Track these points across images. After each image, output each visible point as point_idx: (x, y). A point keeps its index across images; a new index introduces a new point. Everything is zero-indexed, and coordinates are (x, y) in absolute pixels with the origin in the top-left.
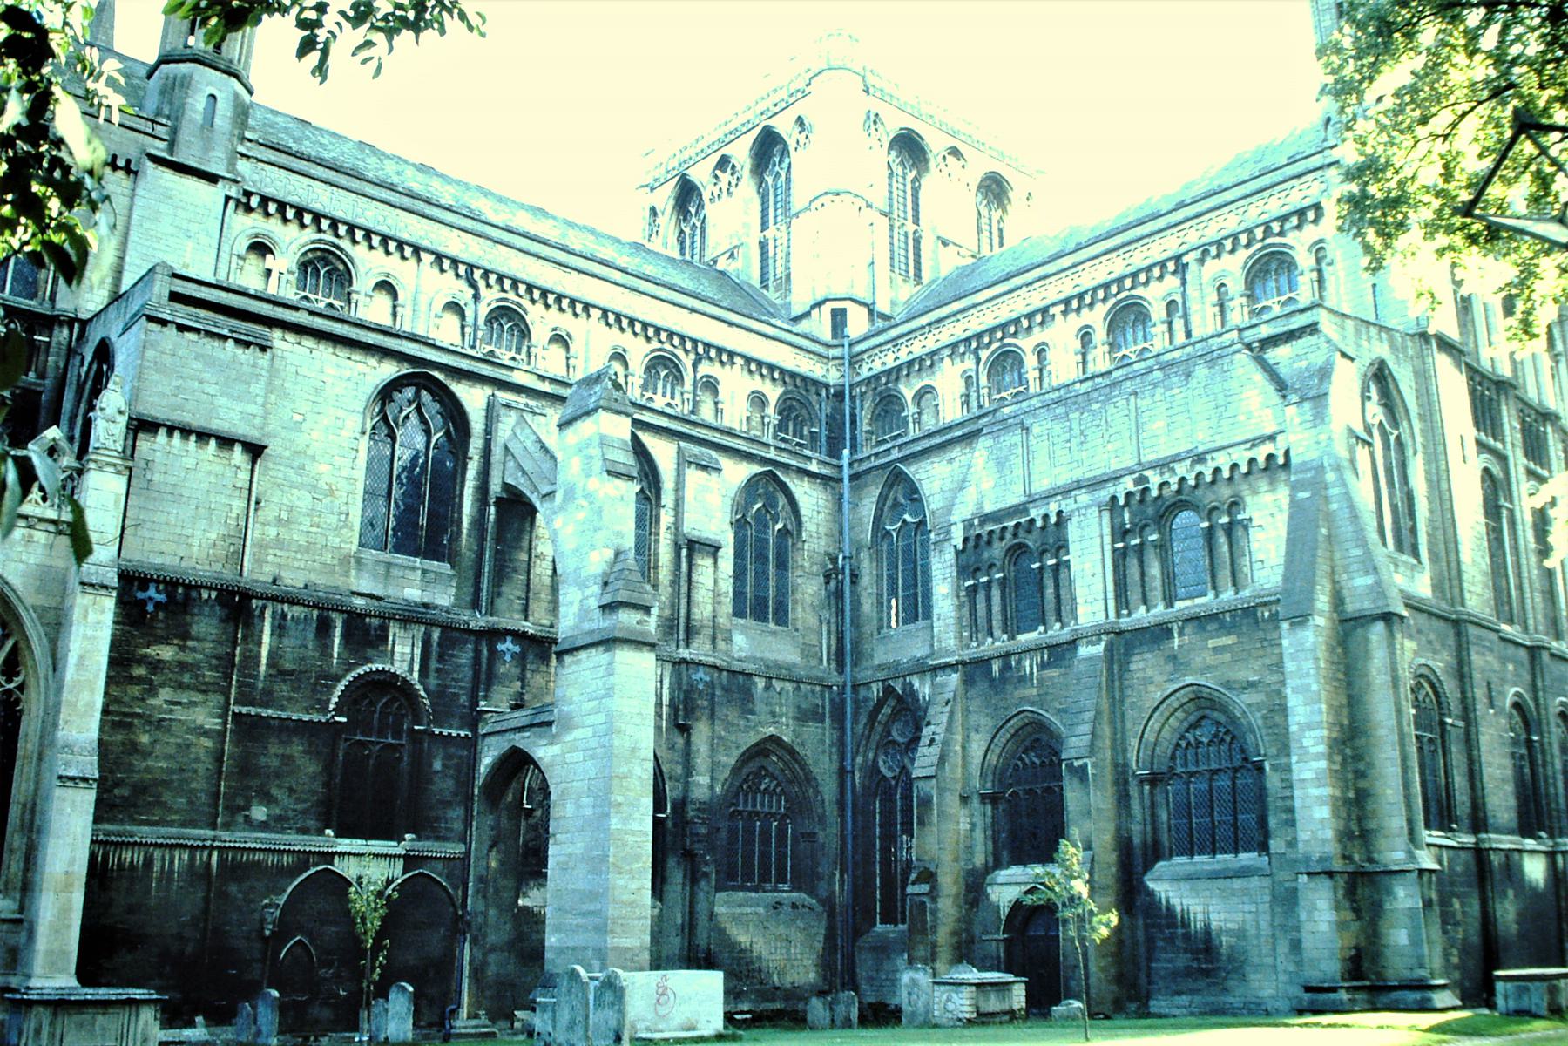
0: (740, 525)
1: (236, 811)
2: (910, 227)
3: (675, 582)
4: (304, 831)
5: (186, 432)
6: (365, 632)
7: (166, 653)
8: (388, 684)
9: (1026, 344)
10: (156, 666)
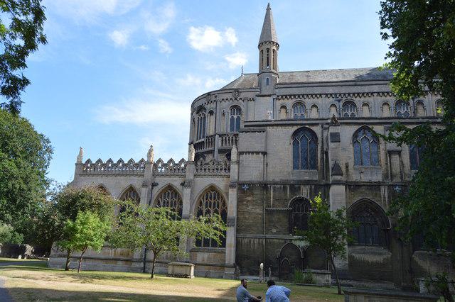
1: (268, 230)
3: (387, 164)
4: (284, 234)
5: (249, 153)
6: (295, 187)
7: (250, 199)
8: (301, 200)
10: (248, 201)
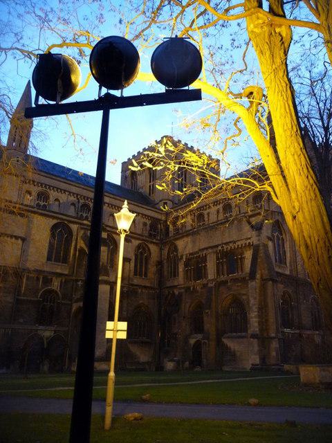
0: (136, 255)
8: (51, 291)
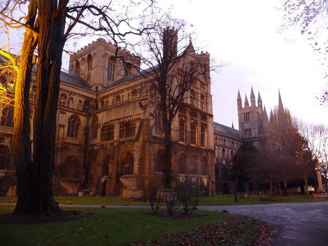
2: (112, 72)
9: (121, 95)
